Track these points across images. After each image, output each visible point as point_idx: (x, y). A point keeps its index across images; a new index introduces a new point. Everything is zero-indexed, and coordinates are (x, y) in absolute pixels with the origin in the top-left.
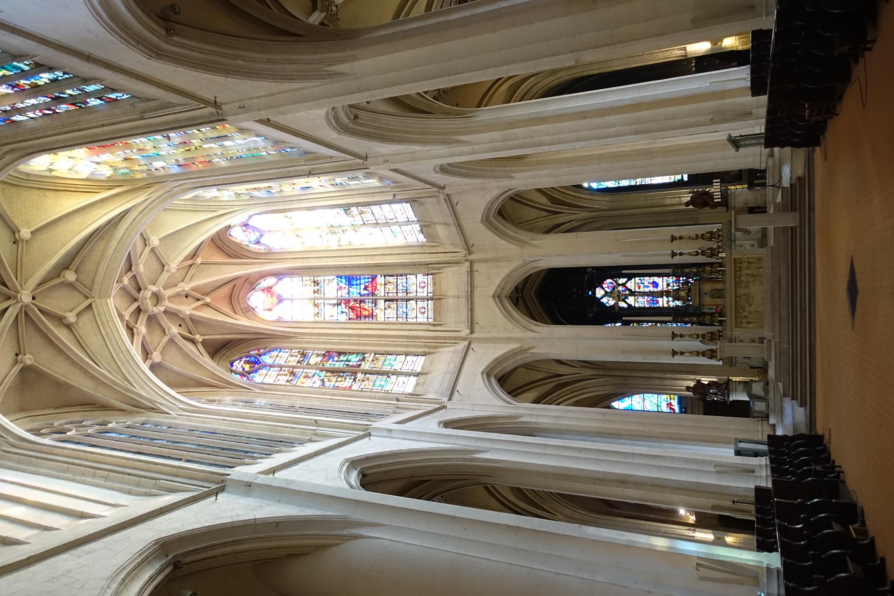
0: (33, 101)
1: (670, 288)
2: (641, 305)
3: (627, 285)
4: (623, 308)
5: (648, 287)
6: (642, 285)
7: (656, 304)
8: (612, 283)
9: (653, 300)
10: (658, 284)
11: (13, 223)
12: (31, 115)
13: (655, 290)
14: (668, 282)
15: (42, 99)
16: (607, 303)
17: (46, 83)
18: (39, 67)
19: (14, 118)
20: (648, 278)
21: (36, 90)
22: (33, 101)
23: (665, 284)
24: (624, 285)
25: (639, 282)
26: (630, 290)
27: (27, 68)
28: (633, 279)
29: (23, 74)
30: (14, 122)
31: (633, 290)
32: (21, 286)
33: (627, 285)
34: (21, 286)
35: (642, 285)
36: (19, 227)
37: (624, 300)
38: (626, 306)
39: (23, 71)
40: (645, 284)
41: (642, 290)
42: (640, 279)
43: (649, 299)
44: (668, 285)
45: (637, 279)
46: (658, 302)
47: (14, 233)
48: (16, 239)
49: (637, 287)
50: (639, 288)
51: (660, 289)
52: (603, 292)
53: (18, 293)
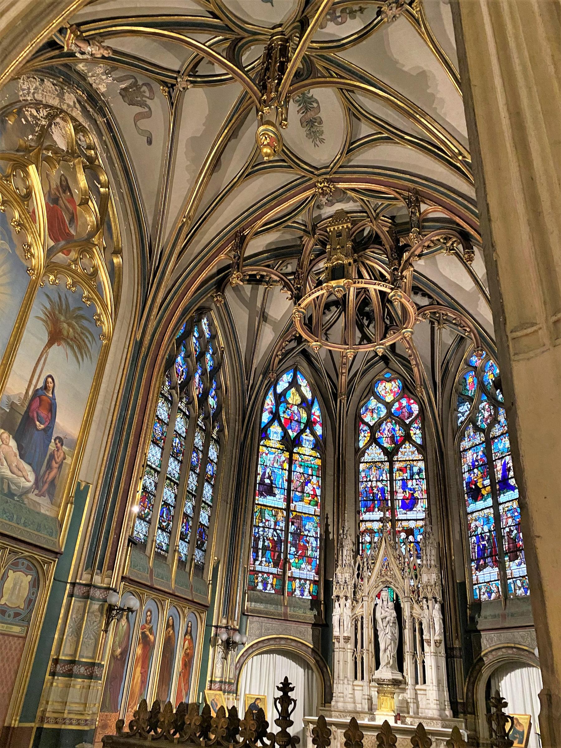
1: (403, 535)
2: (363, 474)
3: (407, 444)
4: (357, 440)
5: (404, 486)
6: (407, 475)
7: (365, 506)
8: (411, 414)
9: (373, 500)
10: (411, 510)
13: (398, 504)
14: (416, 532)
16: (367, 409)
20: (424, 487)
23: (412, 524)
24: (407, 438)
25: (415, 470)
26: (396, 451)
28: (420, 457)
31: (395, 458)
33: (407, 444)
35: (407, 475)
37: (374, 440)
38: (361, 444)
40: (410, 484)
41: (398, 476)
42: (420, 471)
43: (375, 491)
44: (410, 532)
45: (422, 465)
46: (370, 510)
49: (402, 465)
50: (400, 470)
51: (401, 514)
52: (389, 398)
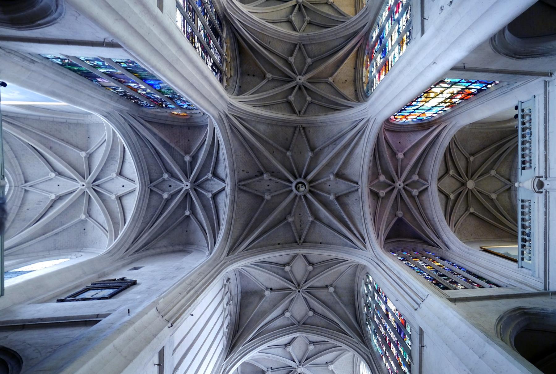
0: (393, 365)
11: (336, 361)
12: (387, 364)
15: (395, 368)
17: (403, 370)
18: (409, 366)
19: (384, 357)
21: (398, 366)
22: (393, 365)
27: (407, 360)
29: (404, 360)
30: (382, 358)
32: (306, 367)
34: (306, 367)
36: (334, 364)
39: (405, 359)
47: (331, 362)
48: (328, 363)
53: (302, 366)
